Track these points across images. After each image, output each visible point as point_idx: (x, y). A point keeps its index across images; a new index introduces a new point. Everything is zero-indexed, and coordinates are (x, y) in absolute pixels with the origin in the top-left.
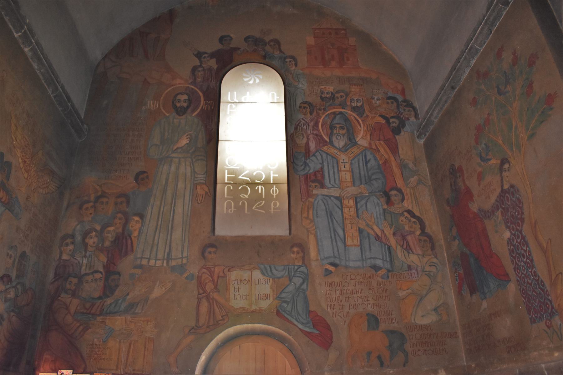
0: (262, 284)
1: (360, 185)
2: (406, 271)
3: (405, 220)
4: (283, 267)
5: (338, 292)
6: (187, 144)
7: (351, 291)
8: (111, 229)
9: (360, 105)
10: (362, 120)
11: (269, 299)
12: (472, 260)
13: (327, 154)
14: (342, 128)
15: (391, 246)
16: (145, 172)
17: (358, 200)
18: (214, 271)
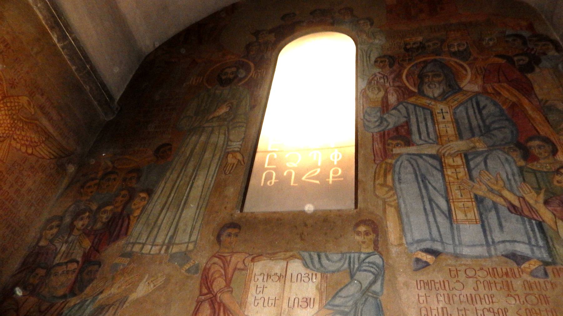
0: (302, 281)
1: (471, 138)
5: (441, 298)
7: (470, 299)
8: (109, 208)
10: (467, 64)
11: (312, 306)
13: (415, 106)
15: (544, 221)
18: (230, 261)
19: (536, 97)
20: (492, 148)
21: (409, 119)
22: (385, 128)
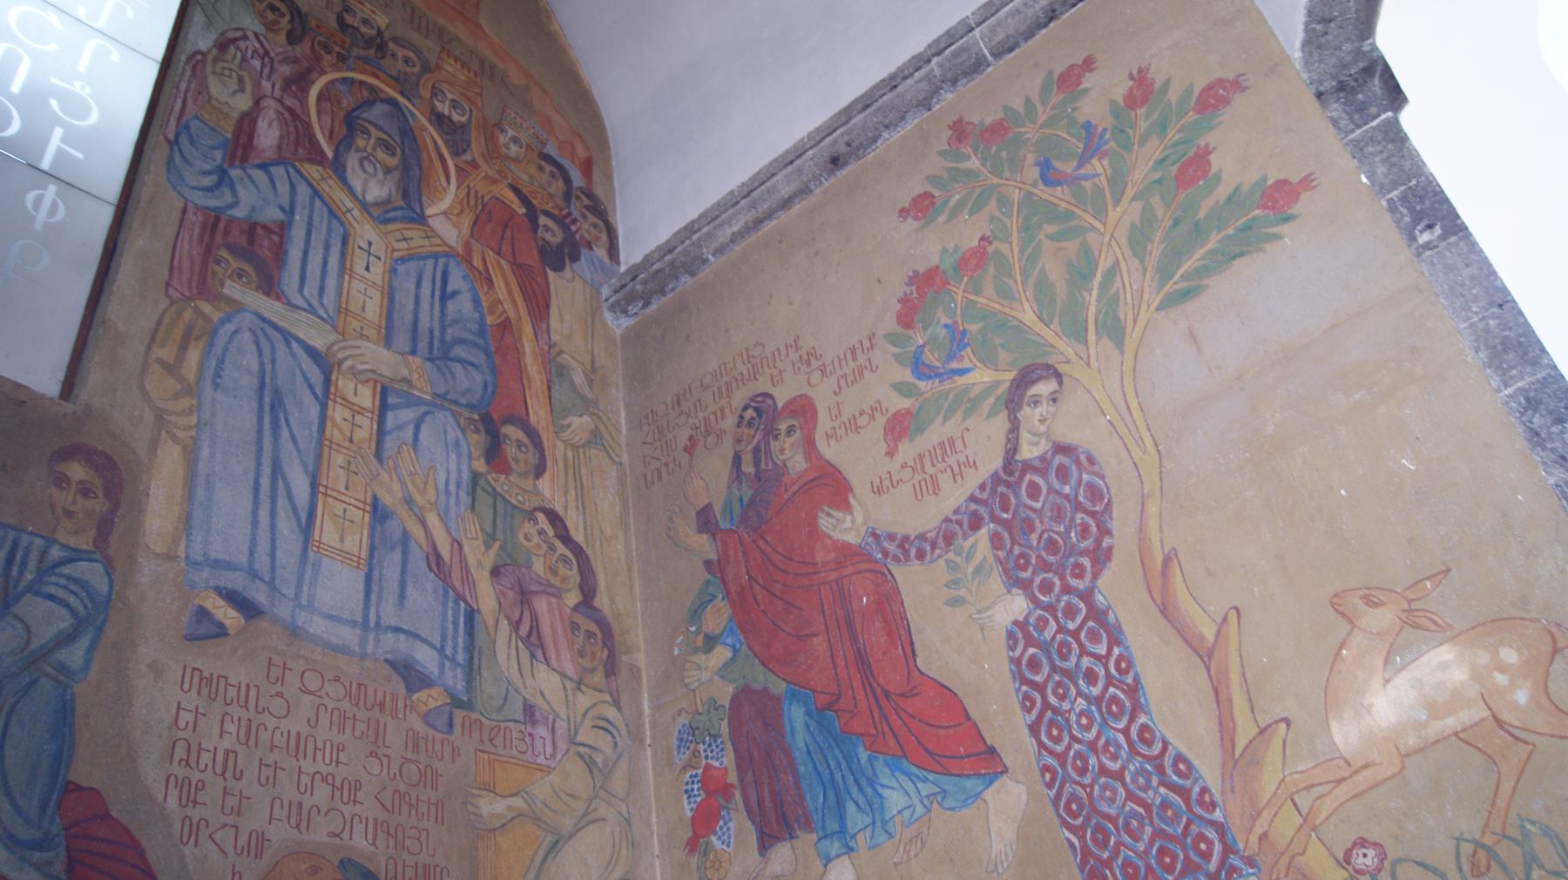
1: (408, 354)
2: (516, 721)
3: (536, 539)
5: (231, 727)
13: (316, 193)
15: (479, 611)
17: (391, 400)
20: (442, 400)
21: (291, 223)
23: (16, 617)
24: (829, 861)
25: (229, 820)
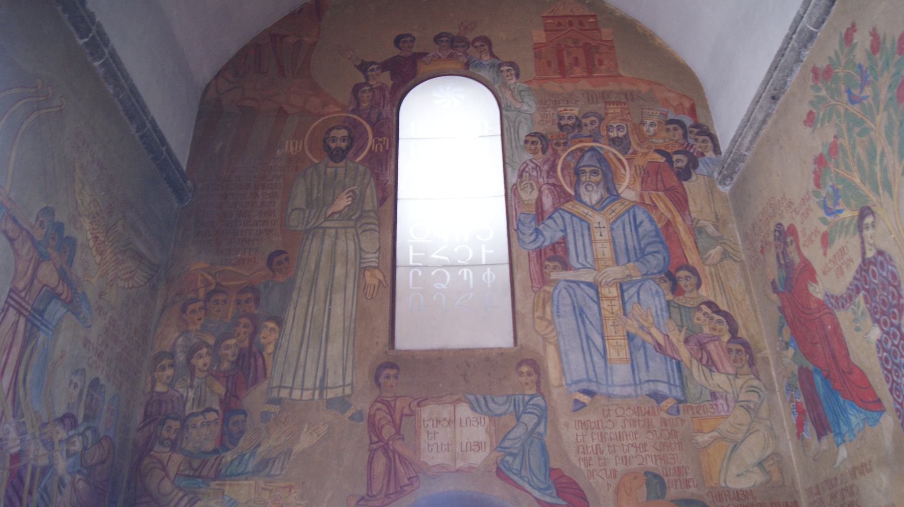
3: (703, 318)
4: (505, 398)
5: (595, 437)
6: (348, 206)
7: (618, 435)
8: (232, 342)
9: (623, 136)
10: (627, 159)
11: (483, 449)
12: (818, 379)
13: (572, 215)
14: (595, 173)
15: (682, 361)
16: (283, 252)
17: (625, 287)
19: (690, 215)
22: (541, 245)
23: (522, 422)
24: (838, 445)
25: (603, 468)
